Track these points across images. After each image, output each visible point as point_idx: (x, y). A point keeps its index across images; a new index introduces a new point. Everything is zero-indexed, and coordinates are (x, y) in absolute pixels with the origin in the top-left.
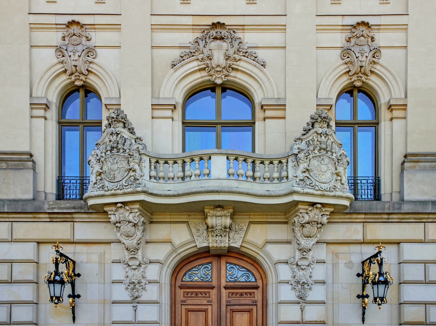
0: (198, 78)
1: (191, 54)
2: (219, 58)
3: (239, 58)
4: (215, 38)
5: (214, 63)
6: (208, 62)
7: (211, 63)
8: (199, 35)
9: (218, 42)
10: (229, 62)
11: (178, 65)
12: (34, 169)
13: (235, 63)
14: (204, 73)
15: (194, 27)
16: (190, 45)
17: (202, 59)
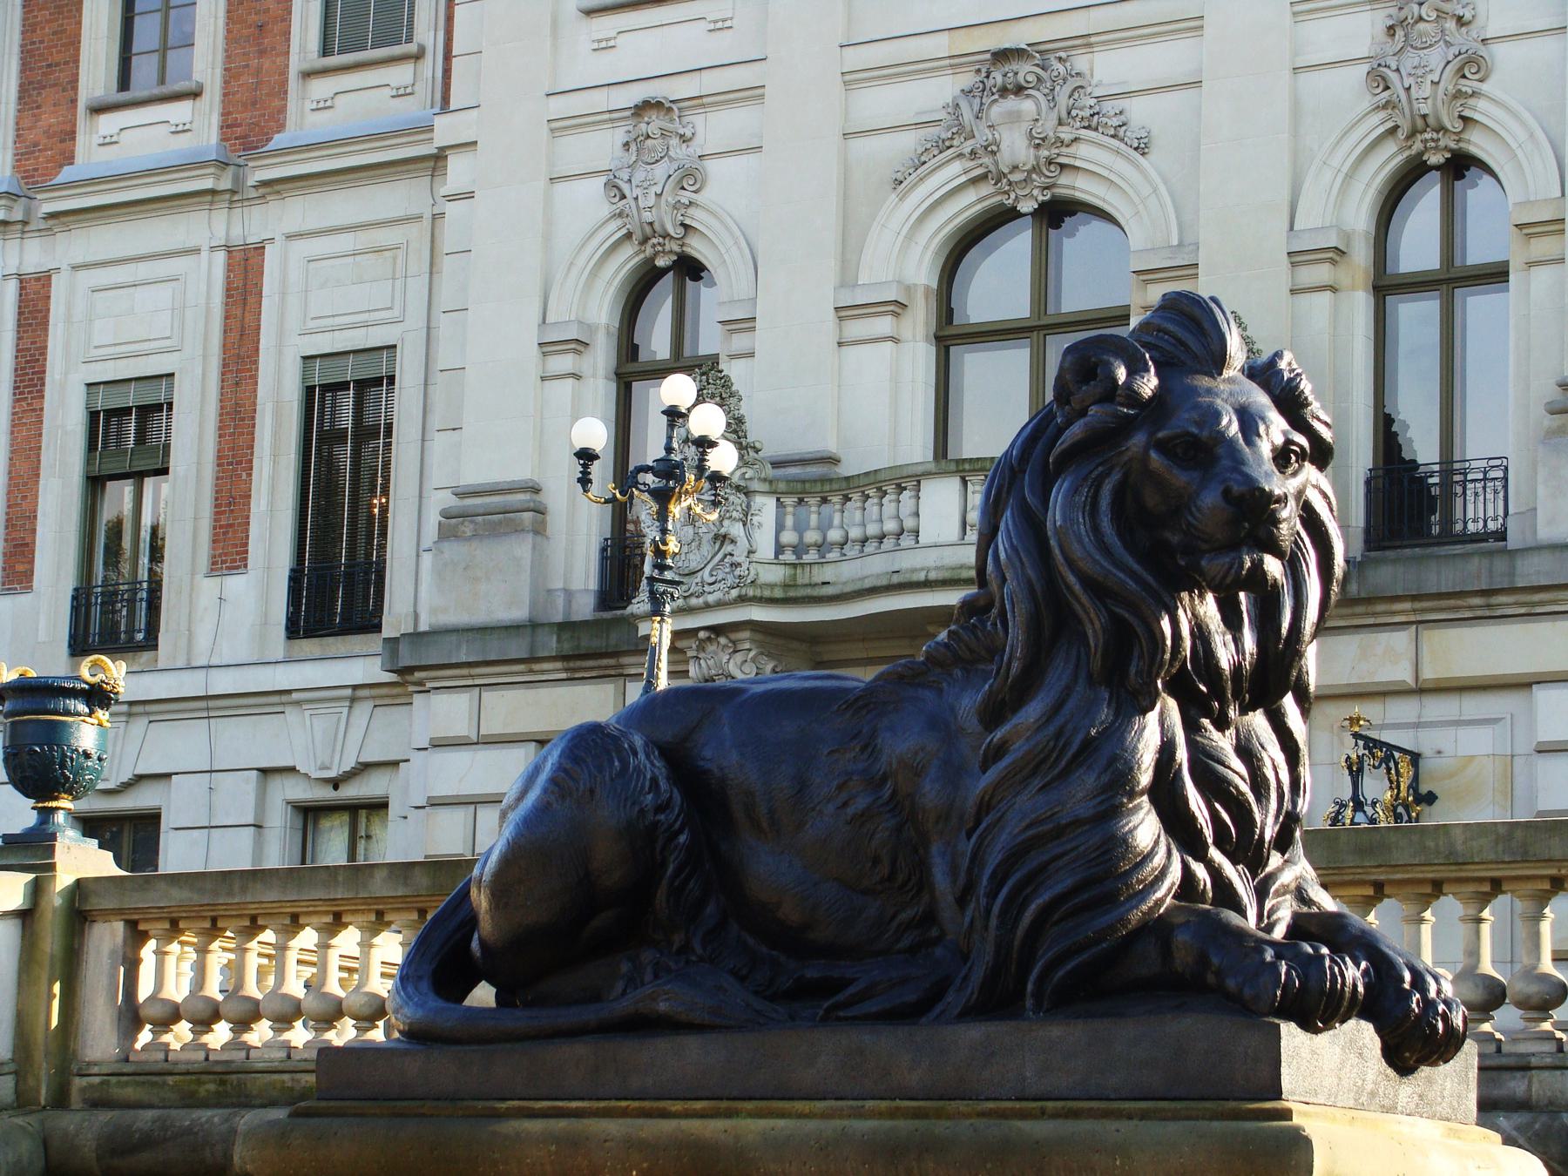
0: (970, 204)
1: (943, 146)
2: (1015, 148)
3: (1072, 137)
4: (1004, 91)
5: (1005, 159)
6: (987, 160)
7: (996, 163)
8: (967, 79)
9: (1011, 103)
10: (1044, 153)
11: (909, 179)
12: (539, 530)
13: (1064, 150)
14: (986, 189)
15: (955, 62)
16: (942, 115)
17: (973, 153)
